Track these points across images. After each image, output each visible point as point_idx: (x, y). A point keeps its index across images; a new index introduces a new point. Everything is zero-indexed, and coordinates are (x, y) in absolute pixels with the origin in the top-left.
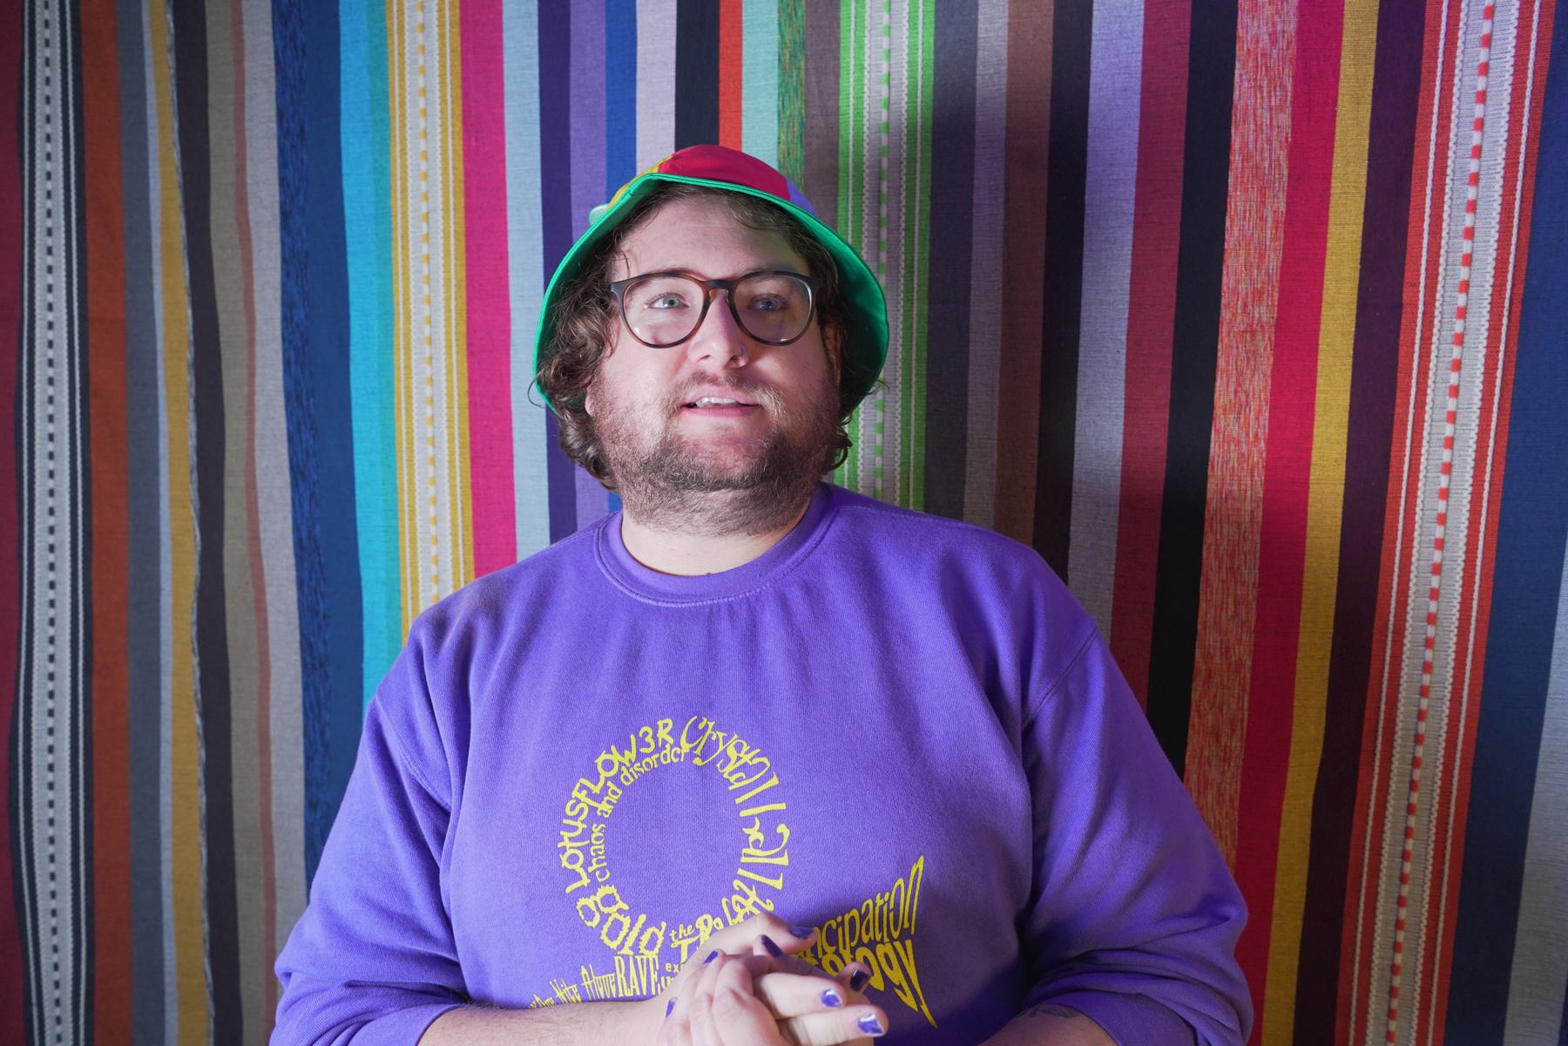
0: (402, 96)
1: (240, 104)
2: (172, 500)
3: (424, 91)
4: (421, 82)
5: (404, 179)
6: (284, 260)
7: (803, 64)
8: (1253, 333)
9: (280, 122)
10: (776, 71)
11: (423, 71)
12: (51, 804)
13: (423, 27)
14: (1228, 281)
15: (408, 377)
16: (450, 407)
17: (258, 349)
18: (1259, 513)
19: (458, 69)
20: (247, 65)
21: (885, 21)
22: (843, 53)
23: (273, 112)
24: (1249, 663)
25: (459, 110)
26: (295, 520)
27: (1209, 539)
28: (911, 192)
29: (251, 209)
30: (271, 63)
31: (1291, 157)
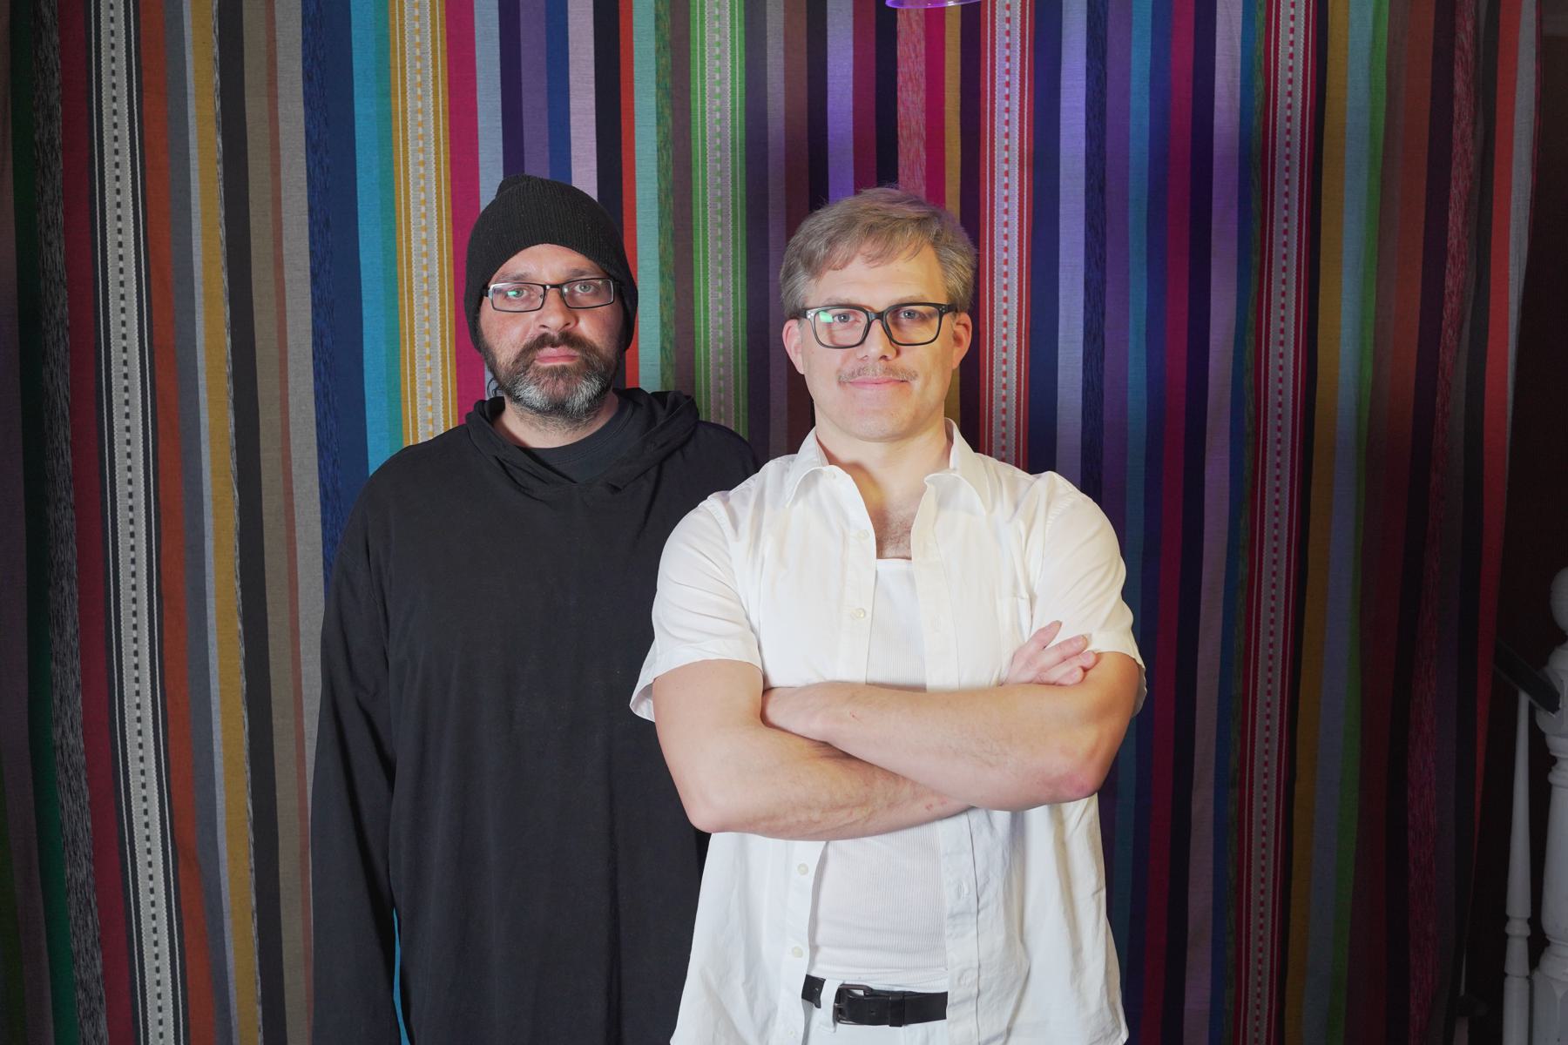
1: (277, 201)
2: (213, 471)
3: (425, 202)
9: (311, 216)
11: (424, 189)
12: (138, 693)
13: (424, 163)
15: (413, 380)
16: (445, 399)
20: (283, 176)
23: (306, 208)
26: (321, 479)
28: (735, 272)
29: (286, 271)
30: (305, 177)
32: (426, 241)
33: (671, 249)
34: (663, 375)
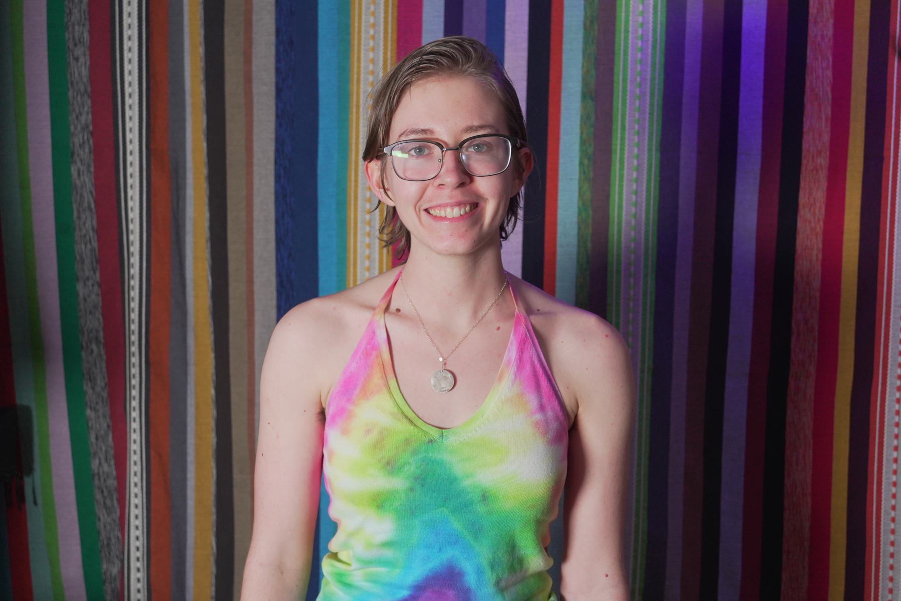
0: (360, 27)
3: (374, 26)
4: (372, 20)
5: (359, 74)
6: (277, 116)
7: (596, 28)
8: (817, 171)
10: (582, 31)
11: (373, 14)
14: (805, 146)
17: (256, 169)
18: (820, 257)
19: (396, 14)
21: (641, 8)
22: (617, 23)
24: (817, 328)
25: (395, 37)
27: (797, 268)
29: (255, 85)
31: (833, 90)
32: (373, 61)
33: (593, 72)
34: (580, 189)
